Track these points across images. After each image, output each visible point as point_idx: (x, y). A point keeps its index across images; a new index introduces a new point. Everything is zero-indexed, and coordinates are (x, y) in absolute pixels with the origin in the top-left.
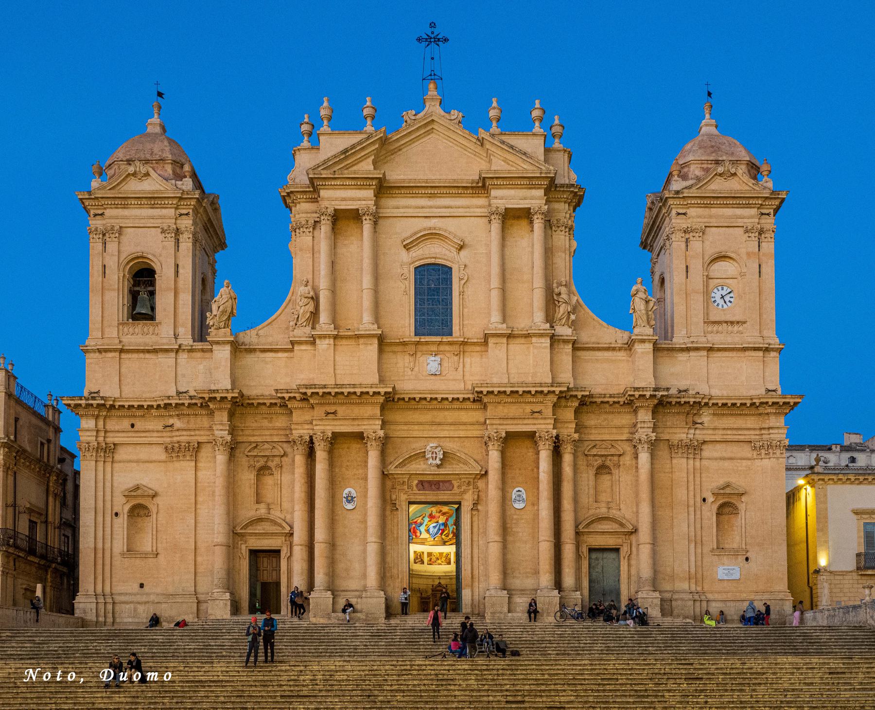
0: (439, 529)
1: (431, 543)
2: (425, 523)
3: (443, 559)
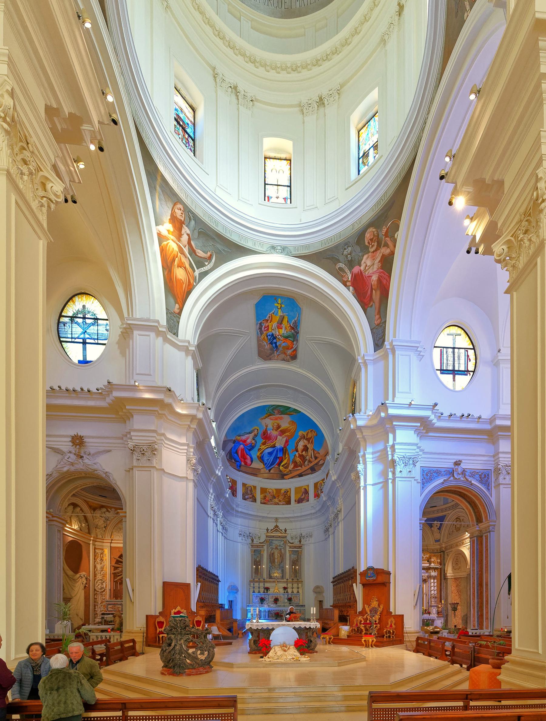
0: (276, 458)
3: (281, 498)
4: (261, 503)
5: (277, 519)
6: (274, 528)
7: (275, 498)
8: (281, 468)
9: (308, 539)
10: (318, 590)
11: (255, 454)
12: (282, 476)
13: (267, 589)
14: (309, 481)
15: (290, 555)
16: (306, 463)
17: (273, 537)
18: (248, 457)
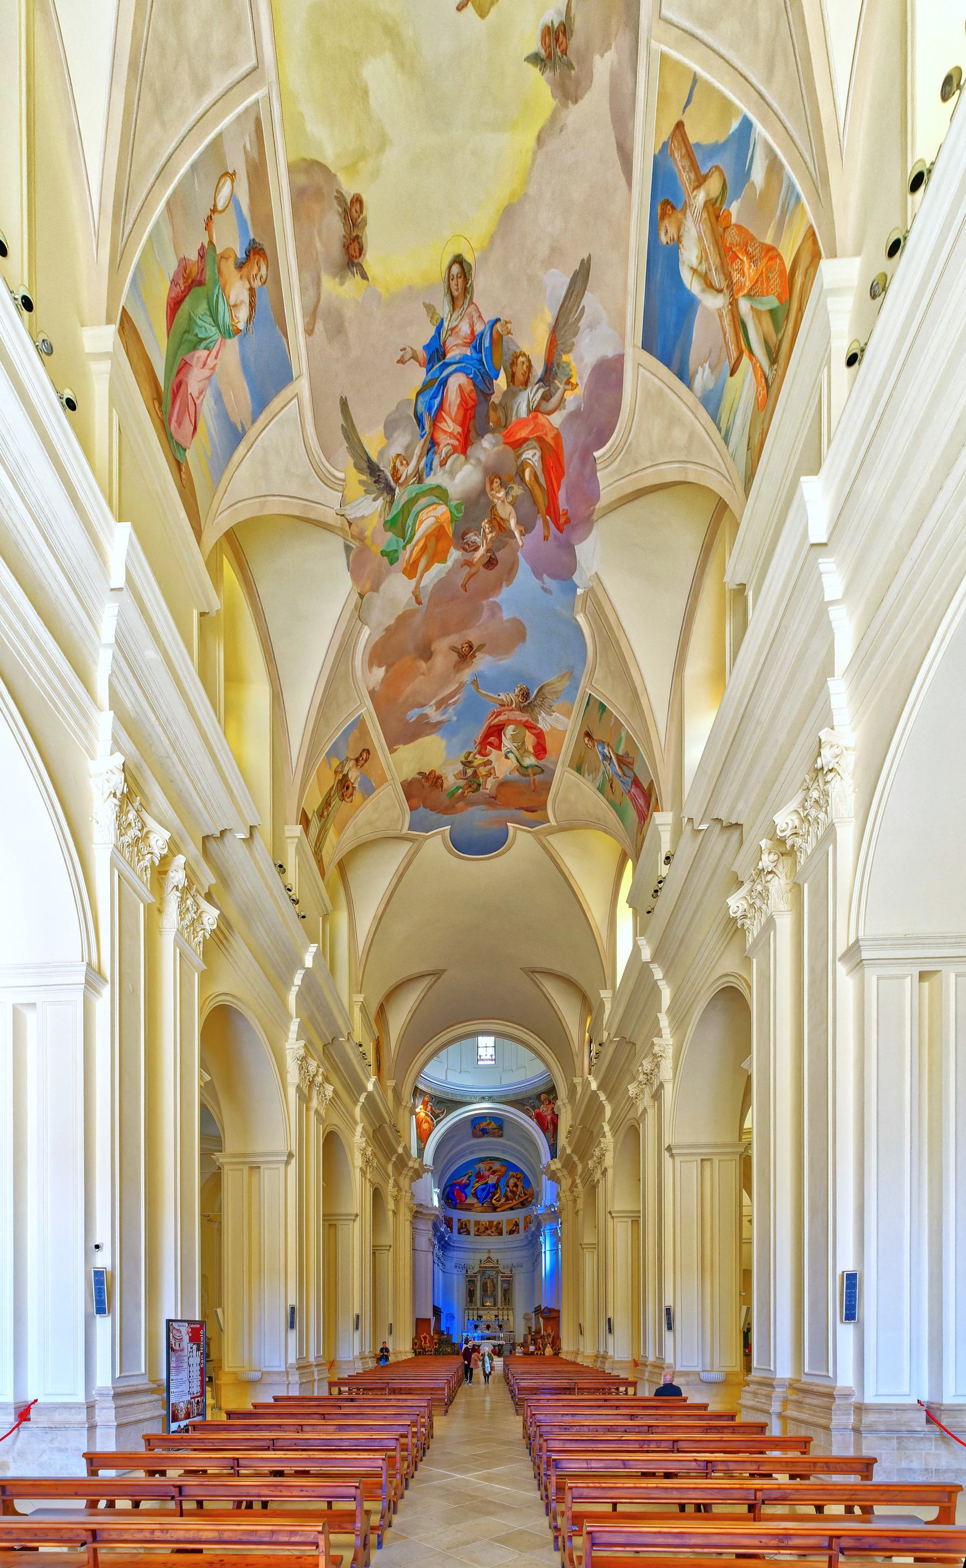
0: (488, 1193)
1: (479, 1209)
3: (493, 1229)
5: (489, 1251)
7: (487, 1229)
8: (494, 1201)
11: (470, 1191)
12: (494, 1209)
13: (480, 1317)
14: (518, 1215)
15: (502, 1285)
16: (517, 1197)
17: (486, 1267)
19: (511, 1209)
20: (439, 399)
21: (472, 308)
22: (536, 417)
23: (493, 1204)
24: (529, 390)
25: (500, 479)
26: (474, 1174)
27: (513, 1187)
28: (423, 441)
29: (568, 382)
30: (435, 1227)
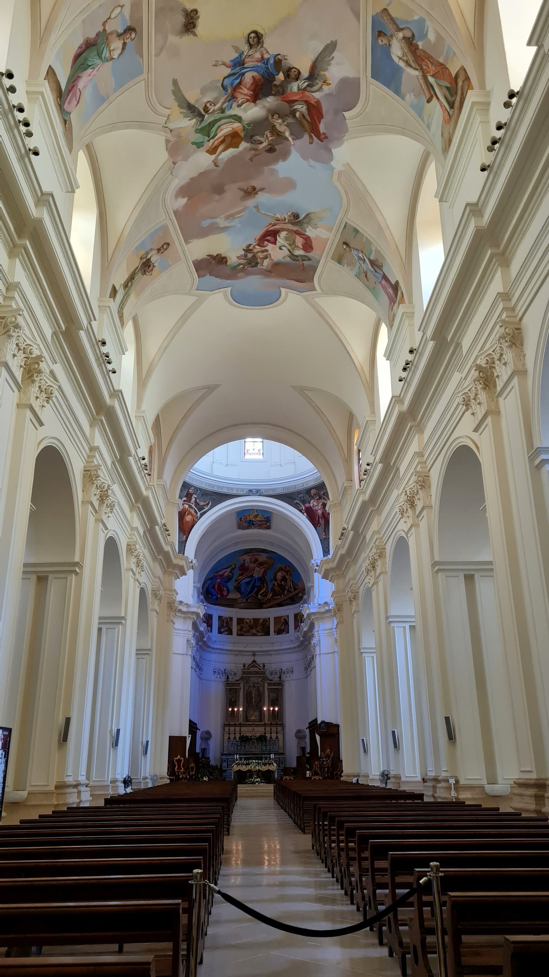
2: (235, 577)
4: (238, 635)
6: (251, 664)
8: (259, 596)
9: (288, 675)
10: (300, 734)
11: (231, 585)
12: (260, 605)
14: (288, 611)
15: (269, 694)
16: (285, 592)
18: (225, 588)
19: (280, 605)
20: (238, 81)
21: (262, 49)
22: (304, 93)
23: (259, 600)
24: (299, 82)
25: (279, 114)
26: (237, 566)
27: (281, 582)
28: (226, 96)
29: (325, 82)
30: (195, 626)
